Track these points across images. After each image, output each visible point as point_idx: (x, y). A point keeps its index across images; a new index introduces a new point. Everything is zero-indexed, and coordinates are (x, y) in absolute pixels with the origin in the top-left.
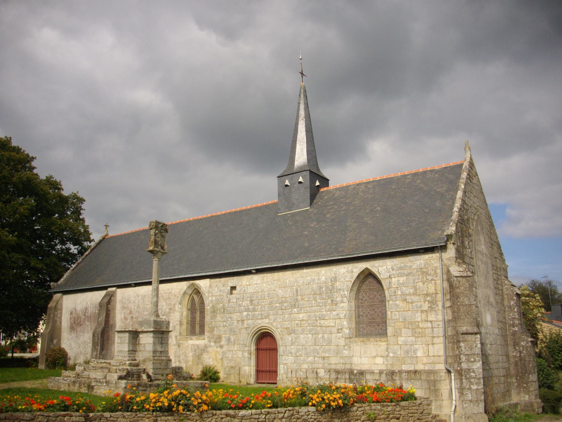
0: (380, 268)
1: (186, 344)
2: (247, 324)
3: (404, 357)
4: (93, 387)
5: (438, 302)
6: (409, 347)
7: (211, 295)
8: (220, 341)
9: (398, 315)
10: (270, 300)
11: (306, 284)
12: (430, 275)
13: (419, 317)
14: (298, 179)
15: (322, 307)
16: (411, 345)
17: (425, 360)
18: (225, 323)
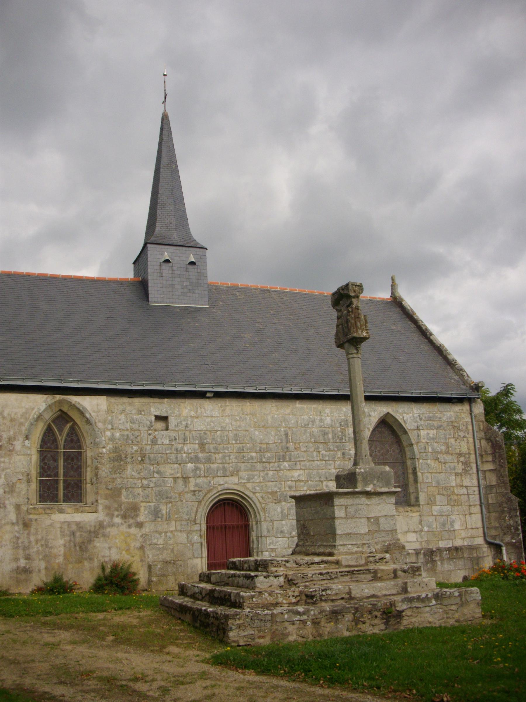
0: (405, 415)
1: (48, 522)
2: (196, 485)
3: (441, 531)
4: (399, 615)
5: (472, 464)
6: (445, 517)
7: (110, 427)
8: (137, 516)
9: (430, 478)
10: (238, 446)
11: (302, 426)
12: (462, 431)
13: (453, 481)
14: (188, 257)
15: (328, 462)
16: (447, 516)
17: (463, 534)
18: (145, 482)
